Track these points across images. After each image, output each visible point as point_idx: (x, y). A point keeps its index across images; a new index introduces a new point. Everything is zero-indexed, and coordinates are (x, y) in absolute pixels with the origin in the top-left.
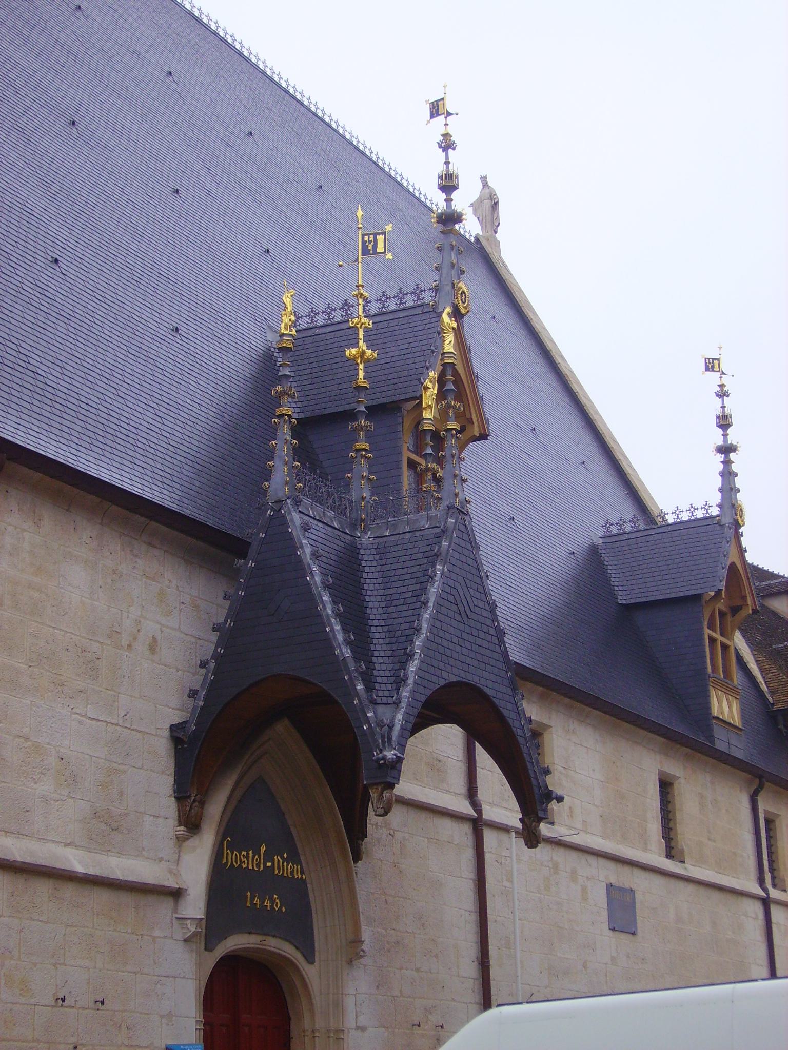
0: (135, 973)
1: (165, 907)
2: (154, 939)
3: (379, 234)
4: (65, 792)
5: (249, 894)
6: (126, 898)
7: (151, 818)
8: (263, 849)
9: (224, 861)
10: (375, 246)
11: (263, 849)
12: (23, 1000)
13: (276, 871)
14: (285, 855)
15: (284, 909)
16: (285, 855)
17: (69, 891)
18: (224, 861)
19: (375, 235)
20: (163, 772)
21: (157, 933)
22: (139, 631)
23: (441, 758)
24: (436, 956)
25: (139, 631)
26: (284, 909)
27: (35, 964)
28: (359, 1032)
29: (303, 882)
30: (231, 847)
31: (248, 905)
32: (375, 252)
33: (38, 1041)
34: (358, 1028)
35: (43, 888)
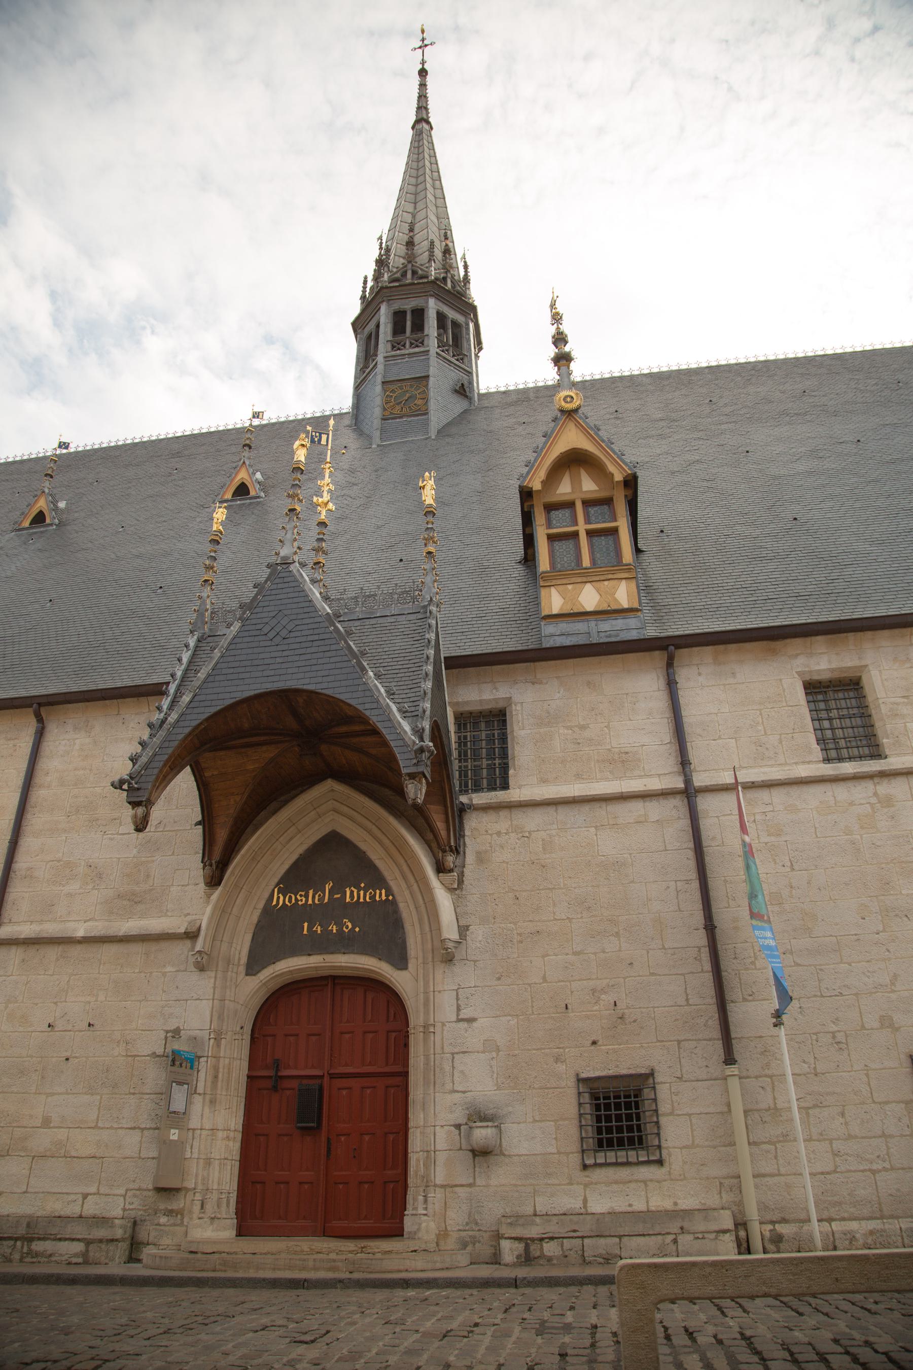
0: (140, 1001)
1: (181, 949)
2: (164, 974)
4: (90, 887)
5: (306, 925)
6: (137, 949)
9: (274, 903)
12: (21, 1029)
13: (348, 900)
14: (362, 885)
17: (76, 951)
18: (274, 903)
23: (626, 750)
24: (617, 934)
26: (357, 929)
27: (37, 1004)
28: (463, 1025)
29: (394, 903)
31: (305, 932)
33: (32, 1057)
34: (459, 1020)
35: (52, 953)
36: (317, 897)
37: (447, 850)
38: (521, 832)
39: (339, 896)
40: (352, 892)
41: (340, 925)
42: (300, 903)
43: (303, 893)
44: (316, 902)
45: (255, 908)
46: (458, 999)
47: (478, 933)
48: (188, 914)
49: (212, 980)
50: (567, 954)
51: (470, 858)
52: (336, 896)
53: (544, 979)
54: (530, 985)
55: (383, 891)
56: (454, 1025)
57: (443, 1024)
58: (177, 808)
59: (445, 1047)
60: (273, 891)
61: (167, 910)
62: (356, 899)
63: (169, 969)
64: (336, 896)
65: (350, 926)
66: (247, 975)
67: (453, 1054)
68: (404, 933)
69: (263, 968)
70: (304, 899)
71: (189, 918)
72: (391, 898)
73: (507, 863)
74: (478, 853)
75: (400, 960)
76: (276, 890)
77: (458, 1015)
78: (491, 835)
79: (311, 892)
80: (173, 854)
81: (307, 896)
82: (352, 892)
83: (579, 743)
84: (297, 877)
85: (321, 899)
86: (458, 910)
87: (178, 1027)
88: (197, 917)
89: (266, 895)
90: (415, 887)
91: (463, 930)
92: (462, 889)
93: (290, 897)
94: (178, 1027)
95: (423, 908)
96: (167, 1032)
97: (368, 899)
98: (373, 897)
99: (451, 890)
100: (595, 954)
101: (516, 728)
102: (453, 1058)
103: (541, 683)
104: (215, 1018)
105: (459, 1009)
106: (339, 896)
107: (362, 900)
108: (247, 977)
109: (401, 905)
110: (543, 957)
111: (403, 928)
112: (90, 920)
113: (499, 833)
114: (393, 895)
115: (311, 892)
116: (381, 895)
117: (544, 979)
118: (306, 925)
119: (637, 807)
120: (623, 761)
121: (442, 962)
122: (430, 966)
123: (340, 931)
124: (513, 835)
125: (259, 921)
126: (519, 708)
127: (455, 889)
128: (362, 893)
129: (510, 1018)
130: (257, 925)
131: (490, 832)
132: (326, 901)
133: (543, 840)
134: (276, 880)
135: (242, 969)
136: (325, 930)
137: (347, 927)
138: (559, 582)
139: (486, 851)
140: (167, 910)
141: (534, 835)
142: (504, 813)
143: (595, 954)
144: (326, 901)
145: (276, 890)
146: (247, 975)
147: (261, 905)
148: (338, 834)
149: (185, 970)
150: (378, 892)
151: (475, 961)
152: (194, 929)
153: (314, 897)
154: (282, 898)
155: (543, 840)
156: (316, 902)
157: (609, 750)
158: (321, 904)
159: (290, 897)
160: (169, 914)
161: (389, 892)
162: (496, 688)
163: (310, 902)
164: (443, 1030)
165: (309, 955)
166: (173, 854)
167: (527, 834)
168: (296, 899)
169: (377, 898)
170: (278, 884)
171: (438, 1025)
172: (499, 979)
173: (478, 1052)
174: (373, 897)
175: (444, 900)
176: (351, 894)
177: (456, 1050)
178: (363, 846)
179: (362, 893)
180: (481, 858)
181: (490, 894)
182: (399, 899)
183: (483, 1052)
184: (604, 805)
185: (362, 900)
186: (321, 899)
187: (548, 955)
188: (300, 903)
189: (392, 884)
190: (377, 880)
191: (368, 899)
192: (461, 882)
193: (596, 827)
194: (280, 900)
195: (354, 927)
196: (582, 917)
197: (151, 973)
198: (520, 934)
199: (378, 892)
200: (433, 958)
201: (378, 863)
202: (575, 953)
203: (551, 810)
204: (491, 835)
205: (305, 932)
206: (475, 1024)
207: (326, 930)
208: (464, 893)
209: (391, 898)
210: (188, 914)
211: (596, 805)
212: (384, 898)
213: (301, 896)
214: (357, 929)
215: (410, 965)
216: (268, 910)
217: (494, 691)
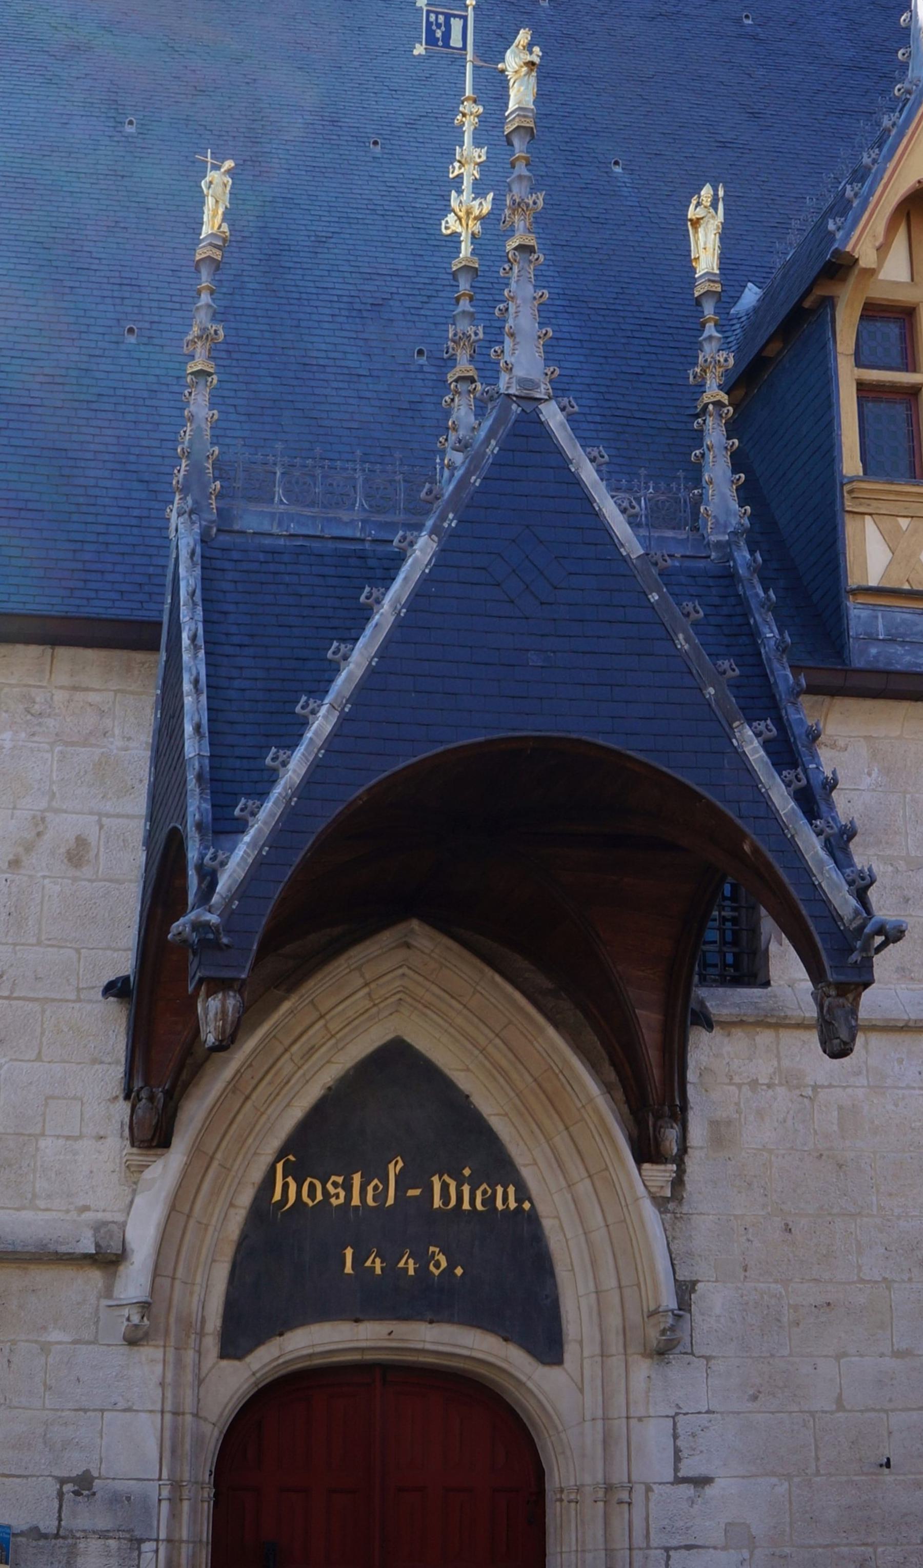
2: (45, 1348)
3: (455, 16)
5: (349, 1252)
7: (61, 1141)
8: (394, 1169)
9: (277, 1196)
10: (447, 35)
11: (394, 1169)
13: (437, 1203)
14: (467, 1172)
16: (467, 1172)
18: (277, 1196)
19: (448, 17)
20: (94, 1061)
21: (55, 1335)
22: (39, 834)
25: (39, 834)
26: (459, 1271)
28: (687, 1490)
30: (297, 1172)
31: (348, 1269)
32: (446, 44)
36: (370, 1189)
38: (798, 1087)
40: (445, 1187)
41: (423, 1259)
42: (334, 1202)
43: (340, 1180)
44: (370, 1201)
46: (675, 1437)
48: (86, 1208)
50: (882, 1355)
51: (697, 1132)
52: (412, 1193)
53: (839, 1401)
54: (812, 1414)
55: (511, 1190)
56: (669, 1489)
57: (649, 1489)
58: (39, 943)
59: (652, 1535)
61: (35, 1196)
63: (55, 1335)
64: (412, 1193)
65: (444, 1264)
66: (223, 1355)
67: (667, 1549)
73: (770, 1151)
74: (715, 1124)
76: (280, 1167)
77: (676, 1469)
78: (739, 1086)
79: (357, 1178)
80: (39, 1058)
81: (347, 1186)
85: (381, 1196)
87: (87, 1472)
88: (108, 1217)
89: (257, 1175)
90: (584, 1188)
92: (680, 1200)
93: (312, 1187)
94: (87, 1472)
95: (600, 1235)
96: (63, 1481)
97: (479, 1207)
98: (489, 1201)
99: (660, 1203)
102: (668, 1557)
104: (167, 1454)
105: (677, 1459)
107: (466, 1206)
108: (224, 1363)
113: (754, 1084)
115: (357, 1178)
116: (505, 1199)
117: (839, 1401)
118: (349, 1252)
122: (616, 1362)
123: (422, 1270)
124: (781, 1091)
125: (244, 1237)
127: (668, 1200)
128: (466, 1189)
129: (774, 1480)
131: (737, 1080)
132: (391, 1201)
136: (391, 1268)
137: (437, 1265)
138: (884, 508)
139: (729, 1123)
140: (35, 1196)
142: (765, 1037)
144: (391, 1201)
145: (280, 1167)
146: (223, 1355)
147: (246, 1198)
148: (409, 1047)
149: (94, 1342)
151: (708, 1358)
156: (370, 1201)
158: (380, 1209)
159: (312, 1187)
160: (41, 1204)
163: (356, 1201)
164: (647, 1499)
165: (357, 1321)
166: (39, 1058)
168: (325, 1192)
169: (499, 1205)
170: (282, 1154)
171: (639, 1490)
172: (754, 1398)
173: (715, 1548)
174: (489, 1201)
176: (444, 1192)
177: (674, 1543)
178: (464, 1082)
179: (466, 1189)
180: (720, 1134)
181: (736, 1216)
183: (725, 1548)
185: (466, 1206)
186: (381, 1196)
187: (845, 1354)
188: (334, 1202)
191: (479, 1207)
192: (678, 1182)
194: (286, 1190)
195: (451, 1266)
196: (910, 1279)
197: (14, 1342)
198: (796, 1308)
199: (500, 1190)
201: (498, 1125)
202: (898, 1354)
204: (739, 1086)
205: (348, 1269)
206: (709, 1491)
208: (685, 1209)
209: (527, 1206)
210: (86, 1208)
212: (513, 1205)
213: (335, 1185)
214: (459, 1271)
216: (262, 1211)
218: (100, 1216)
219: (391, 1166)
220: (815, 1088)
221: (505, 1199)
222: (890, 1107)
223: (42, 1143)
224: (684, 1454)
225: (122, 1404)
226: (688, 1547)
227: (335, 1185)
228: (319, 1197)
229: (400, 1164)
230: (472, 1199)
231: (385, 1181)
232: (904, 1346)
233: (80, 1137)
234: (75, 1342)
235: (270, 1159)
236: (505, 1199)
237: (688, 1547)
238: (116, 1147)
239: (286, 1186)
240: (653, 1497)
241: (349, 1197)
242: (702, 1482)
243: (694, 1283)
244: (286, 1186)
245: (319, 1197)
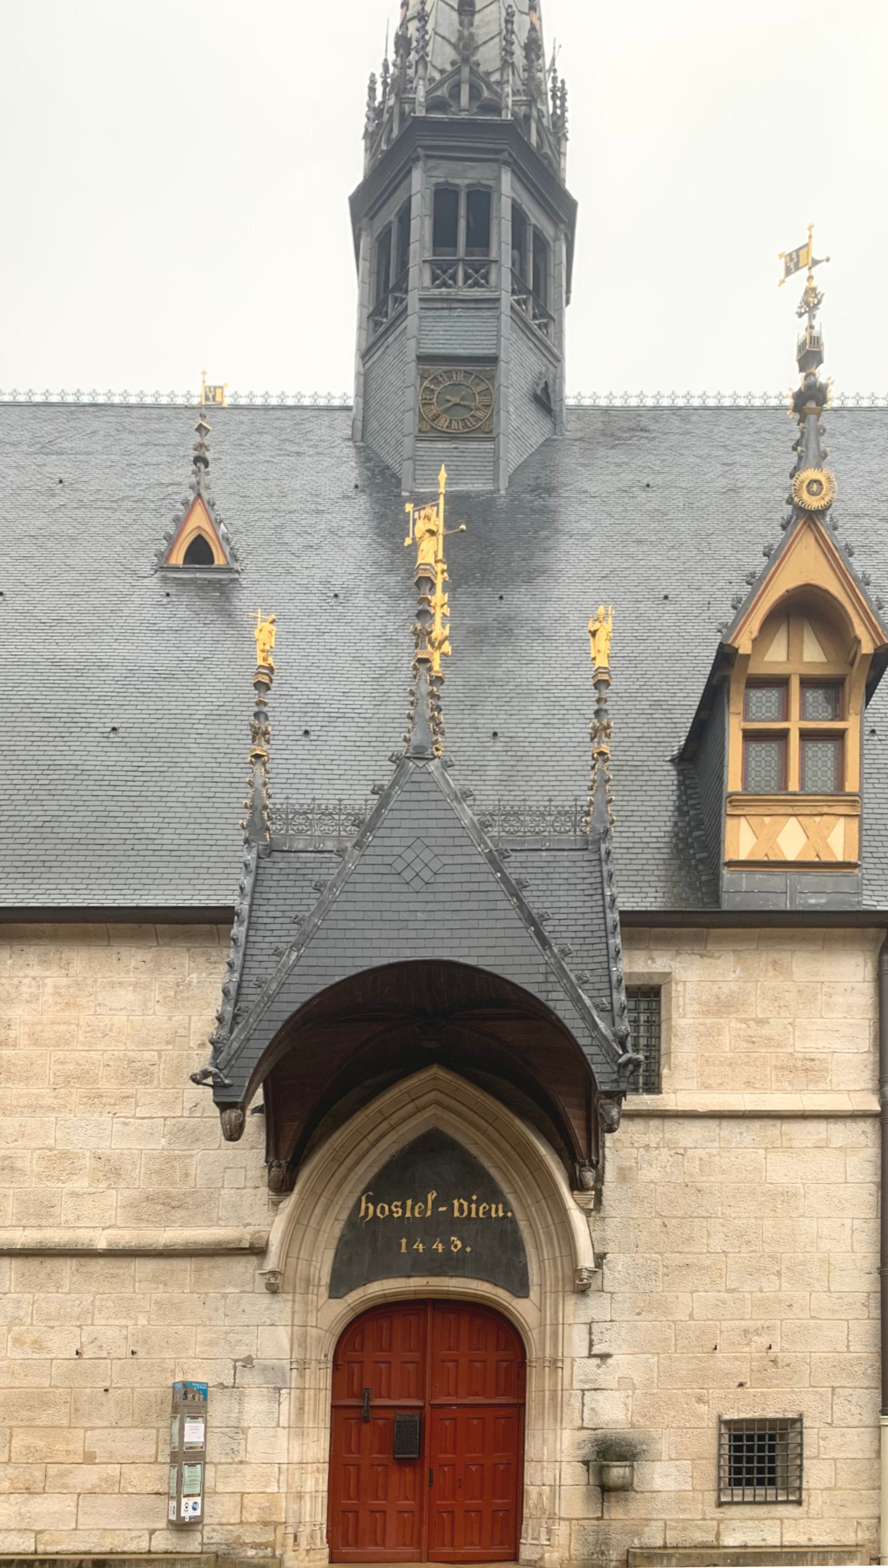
2: (224, 1296)
5: (404, 1241)
8: (431, 1196)
9: (362, 1213)
11: (431, 1196)
13: (456, 1214)
14: (474, 1197)
15: (468, 1249)
17: (97, 1266)
18: (362, 1213)
26: (468, 1249)
29: (513, 1221)
31: (403, 1250)
34: (591, 1356)
36: (417, 1208)
37: (582, 1160)
39: (444, 1209)
40: (461, 1205)
41: (447, 1243)
42: (396, 1215)
43: (399, 1204)
45: (336, 1219)
46: (590, 1333)
47: (618, 1264)
48: (249, 1224)
49: (290, 1304)
51: (610, 1174)
52: (441, 1209)
53: (691, 1316)
55: (500, 1206)
57: (573, 1360)
60: (360, 1200)
61: (219, 1219)
62: (465, 1214)
63: (230, 1290)
64: (441, 1209)
65: (460, 1245)
67: (583, 1390)
68: (525, 1256)
69: (351, 1290)
70: (400, 1211)
71: (251, 1229)
72: (509, 1214)
73: (656, 1183)
75: (521, 1289)
76: (364, 1198)
77: (590, 1350)
78: (638, 1148)
79: (409, 1203)
82: (461, 1205)
83: (753, 1042)
84: (389, 1183)
86: (593, 1234)
89: (351, 1204)
91: (600, 1258)
93: (383, 1208)
97: (481, 1215)
98: (487, 1213)
100: (751, 1292)
101: (674, 1015)
103: (712, 957)
105: (591, 1344)
106: (444, 1209)
107: (473, 1215)
109: (523, 1225)
110: (692, 1292)
111: (524, 1251)
112: (110, 1227)
113: (647, 1147)
114: (512, 1211)
115: (409, 1203)
116: (496, 1211)
117: (691, 1316)
118: (404, 1241)
119: (818, 1129)
120: (809, 1070)
121: (574, 1292)
123: (447, 1250)
125: (343, 1236)
126: (680, 988)
127: (592, 1210)
128: (474, 1206)
130: (340, 1239)
131: (636, 1145)
132: (429, 1213)
133: (701, 1159)
134: (362, 1187)
135: (324, 1291)
136: (428, 1250)
137: (456, 1246)
139: (631, 1168)
140: (219, 1219)
141: (690, 1153)
142: (654, 1123)
143: (751, 1292)
144: (429, 1213)
145: (364, 1198)
147: (344, 1216)
149: (253, 1292)
150: (494, 1206)
152: (262, 1243)
153: (413, 1209)
154: (371, 1208)
155: (701, 1159)
156: (417, 1215)
157: (791, 1054)
158: (423, 1218)
161: (507, 1207)
162: (653, 959)
163: (408, 1215)
164: (572, 1366)
167: (682, 1151)
168: (390, 1210)
169: (493, 1215)
170: (364, 1192)
171: (567, 1362)
172: (639, 1314)
174: (487, 1213)
175: (578, 1219)
177: (587, 1387)
179: (474, 1206)
180: (624, 1175)
182: (519, 1216)
183: (617, 1390)
184: (778, 1123)
186: (423, 1212)
187: (697, 1291)
188: (396, 1215)
189: (511, 1198)
190: (493, 1194)
193: (766, 1149)
198: (667, 1267)
199: (494, 1206)
200: (564, 1287)
202: (728, 1291)
203: (713, 1124)
204: (638, 1148)
205: (403, 1250)
207: (430, 1248)
209: (509, 1214)
210: (249, 1224)
211: (769, 1123)
212: (501, 1214)
213: (396, 1206)
215: (532, 1294)
216: (353, 1222)
217: (649, 962)
218: (257, 1227)
219: (429, 1196)
220: (685, 1149)
221: (497, 1211)
222: (733, 1159)
223: (223, 1192)
224: (596, 1342)
225: (268, 1322)
226: (596, 1390)
227: (396, 1206)
228: (387, 1213)
229: (435, 1194)
230: (478, 1211)
231: (425, 1203)
232: (733, 1287)
233: (244, 1188)
234: (242, 1292)
235: (357, 1195)
236: (497, 1211)
237: (596, 1390)
238: (264, 1192)
239: (367, 1208)
240: (576, 1364)
241: (404, 1213)
242: (604, 1357)
243: (605, 1254)
244: (367, 1208)
245: (387, 1213)
